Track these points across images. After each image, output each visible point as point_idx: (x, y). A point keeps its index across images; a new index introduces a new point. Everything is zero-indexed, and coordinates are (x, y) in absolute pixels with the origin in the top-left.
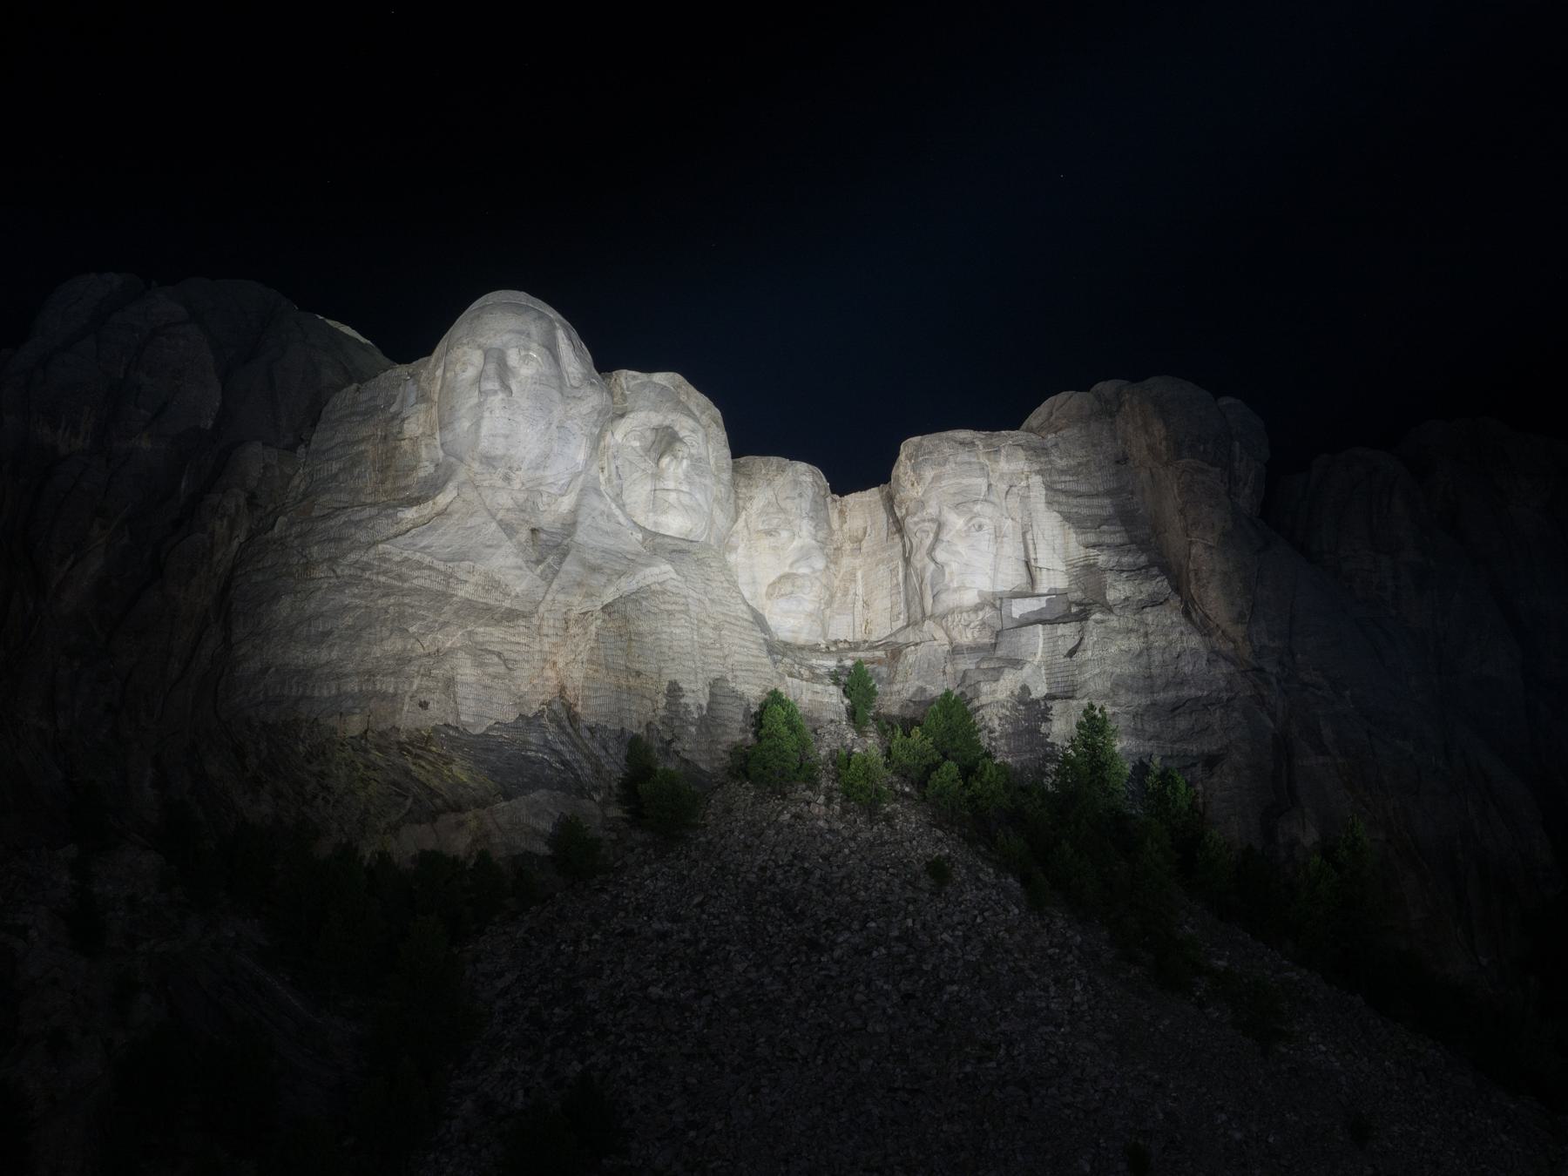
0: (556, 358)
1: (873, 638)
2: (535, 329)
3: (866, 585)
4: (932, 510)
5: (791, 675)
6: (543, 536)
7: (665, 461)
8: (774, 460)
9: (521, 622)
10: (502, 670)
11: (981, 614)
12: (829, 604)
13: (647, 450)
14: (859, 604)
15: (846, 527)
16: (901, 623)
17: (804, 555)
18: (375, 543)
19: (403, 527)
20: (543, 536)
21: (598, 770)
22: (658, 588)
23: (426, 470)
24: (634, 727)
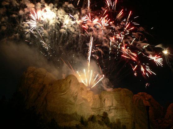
17: (92, 100)
21: (78, 119)
24: (82, 115)
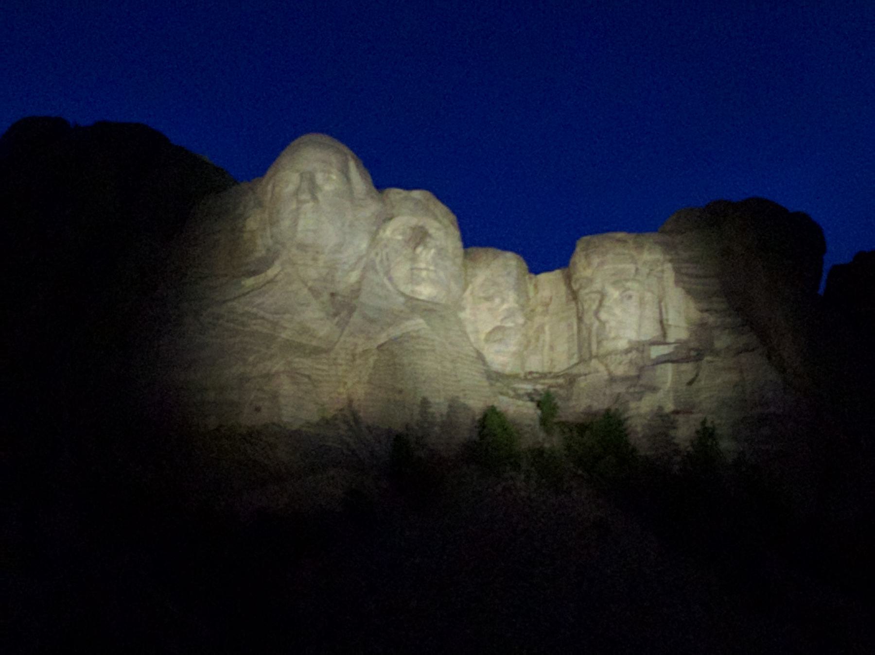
0: (348, 180)
1: (556, 370)
2: (334, 159)
3: (551, 335)
4: (597, 286)
5: (502, 394)
6: (339, 298)
7: (419, 249)
8: (491, 251)
9: (324, 355)
10: (310, 387)
11: (630, 355)
12: (527, 347)
13: (407, 242)
14: (547, 348)
15: (539, 296)
16: (575, 360)
17: (510, 314)
18: (225, 302)
19: (246, 291)
20: (339, 298)
22: (414, 334)
23: (260, 253)
